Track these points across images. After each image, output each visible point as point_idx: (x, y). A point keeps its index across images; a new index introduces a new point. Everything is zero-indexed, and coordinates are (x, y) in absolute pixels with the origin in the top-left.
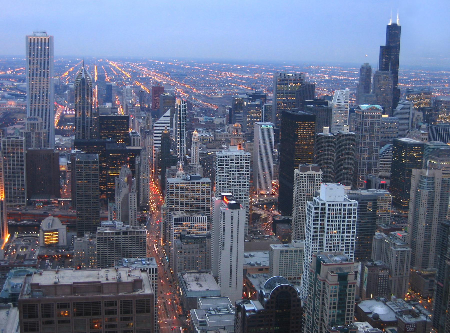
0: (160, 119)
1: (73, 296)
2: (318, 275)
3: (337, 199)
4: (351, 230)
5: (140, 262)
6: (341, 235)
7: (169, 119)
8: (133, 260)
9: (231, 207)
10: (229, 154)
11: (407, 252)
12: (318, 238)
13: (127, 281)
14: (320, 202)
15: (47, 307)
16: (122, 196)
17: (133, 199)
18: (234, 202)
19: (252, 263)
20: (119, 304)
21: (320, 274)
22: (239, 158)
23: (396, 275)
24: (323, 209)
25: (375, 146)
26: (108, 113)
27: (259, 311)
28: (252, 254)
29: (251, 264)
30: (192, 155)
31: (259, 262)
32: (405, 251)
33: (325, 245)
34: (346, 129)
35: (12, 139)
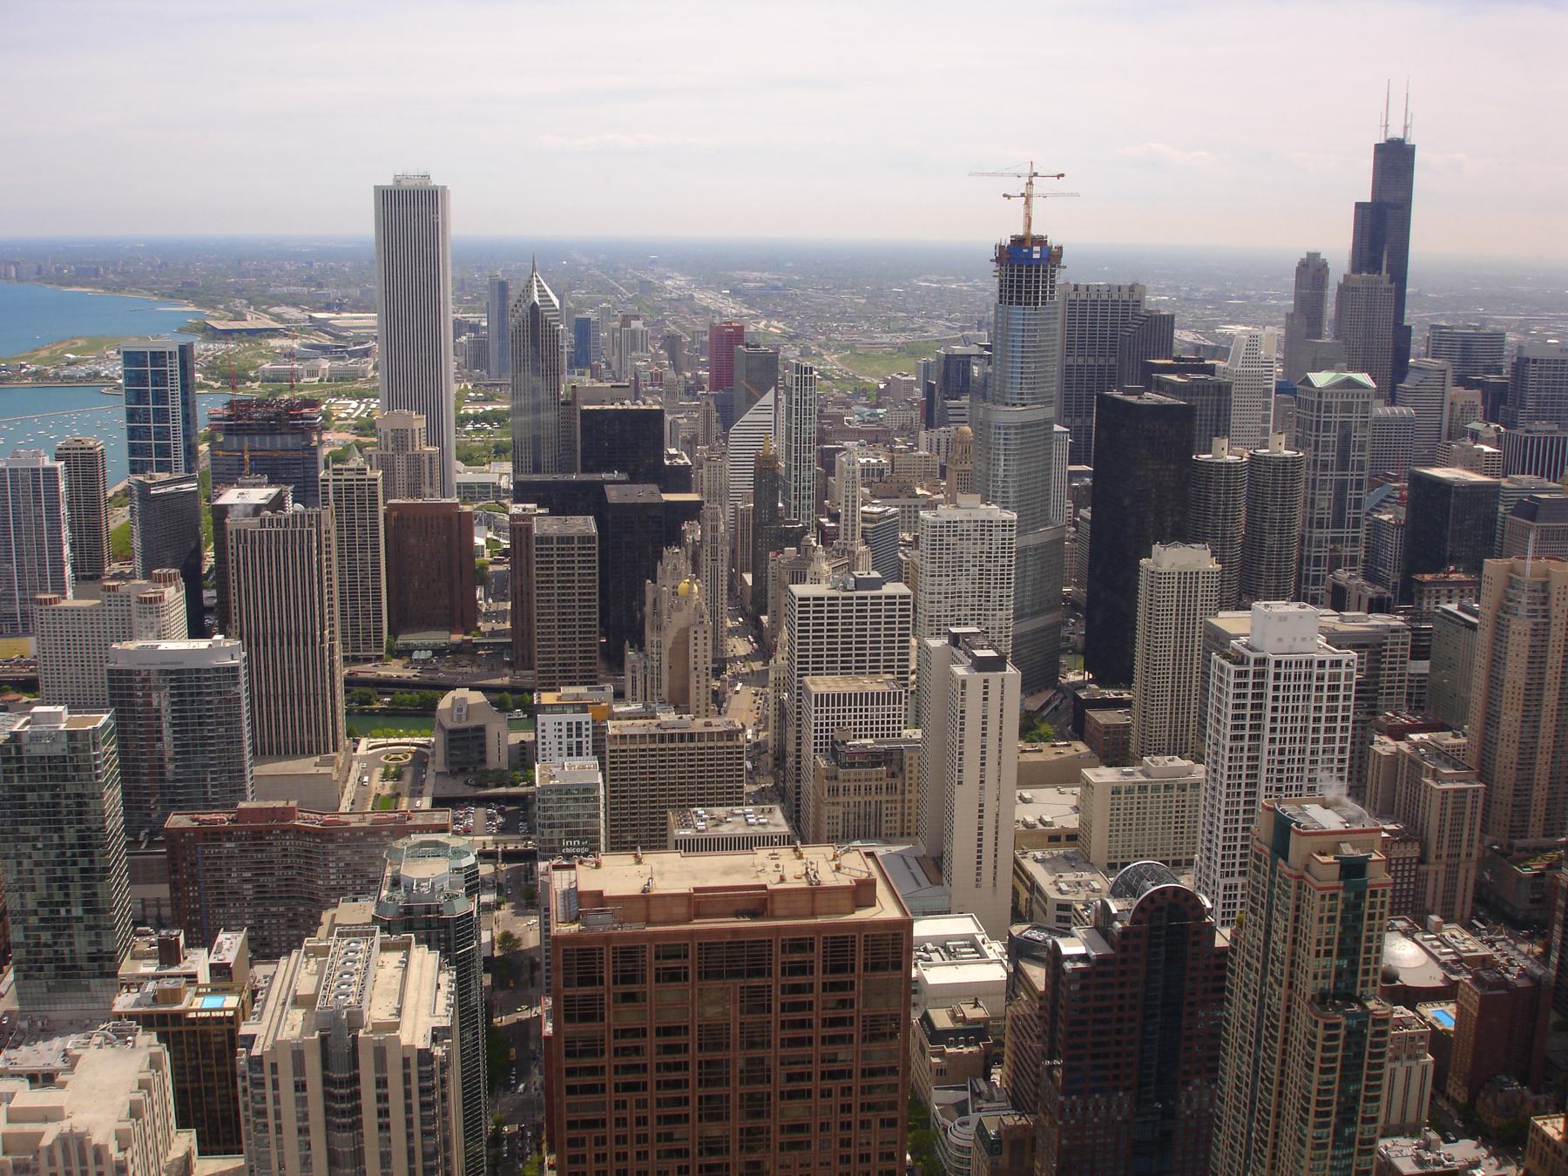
0: (746, 417)
1: (698, 925)
2: (1280, 861)
3: (1299, 647)
4: (1338, 735)
5: (741, 819)
6: (1309, 747)
7: (771, 418)
8: (719, 811)
9: (982, 665)
10: (958, 515)
11: (1470, 793)
12: (1246, 754)
13: (836, 884)
14: (1253, 656)
15: (629, 953)
16: (670, 635)
17: (700, 642)
18: (991, 653)
19: (1030, 819)
20: (819, 947)
21: (1286, 859)
22: (986, 526)
23: (1438, 857)
24: (1260, 674)
25: (1351, 494)
26: (603, 402)
27: (1101, 960)
28: (1027, 794)
29: (1026, 824)
30: (843, 517)
31: (1047, 819)
32: (1465, 790)
33: (1264, 775)
34: (1280, 448)
35: (346, 475)
